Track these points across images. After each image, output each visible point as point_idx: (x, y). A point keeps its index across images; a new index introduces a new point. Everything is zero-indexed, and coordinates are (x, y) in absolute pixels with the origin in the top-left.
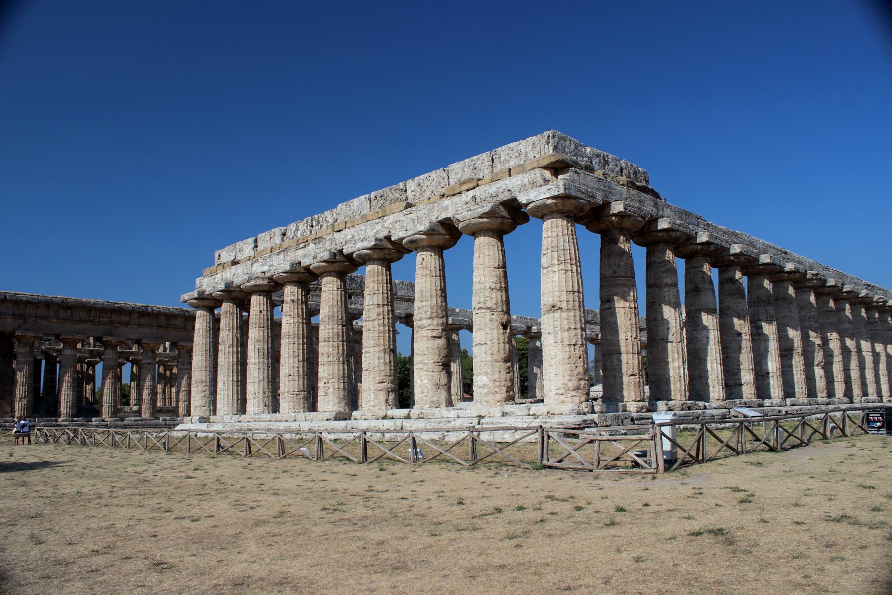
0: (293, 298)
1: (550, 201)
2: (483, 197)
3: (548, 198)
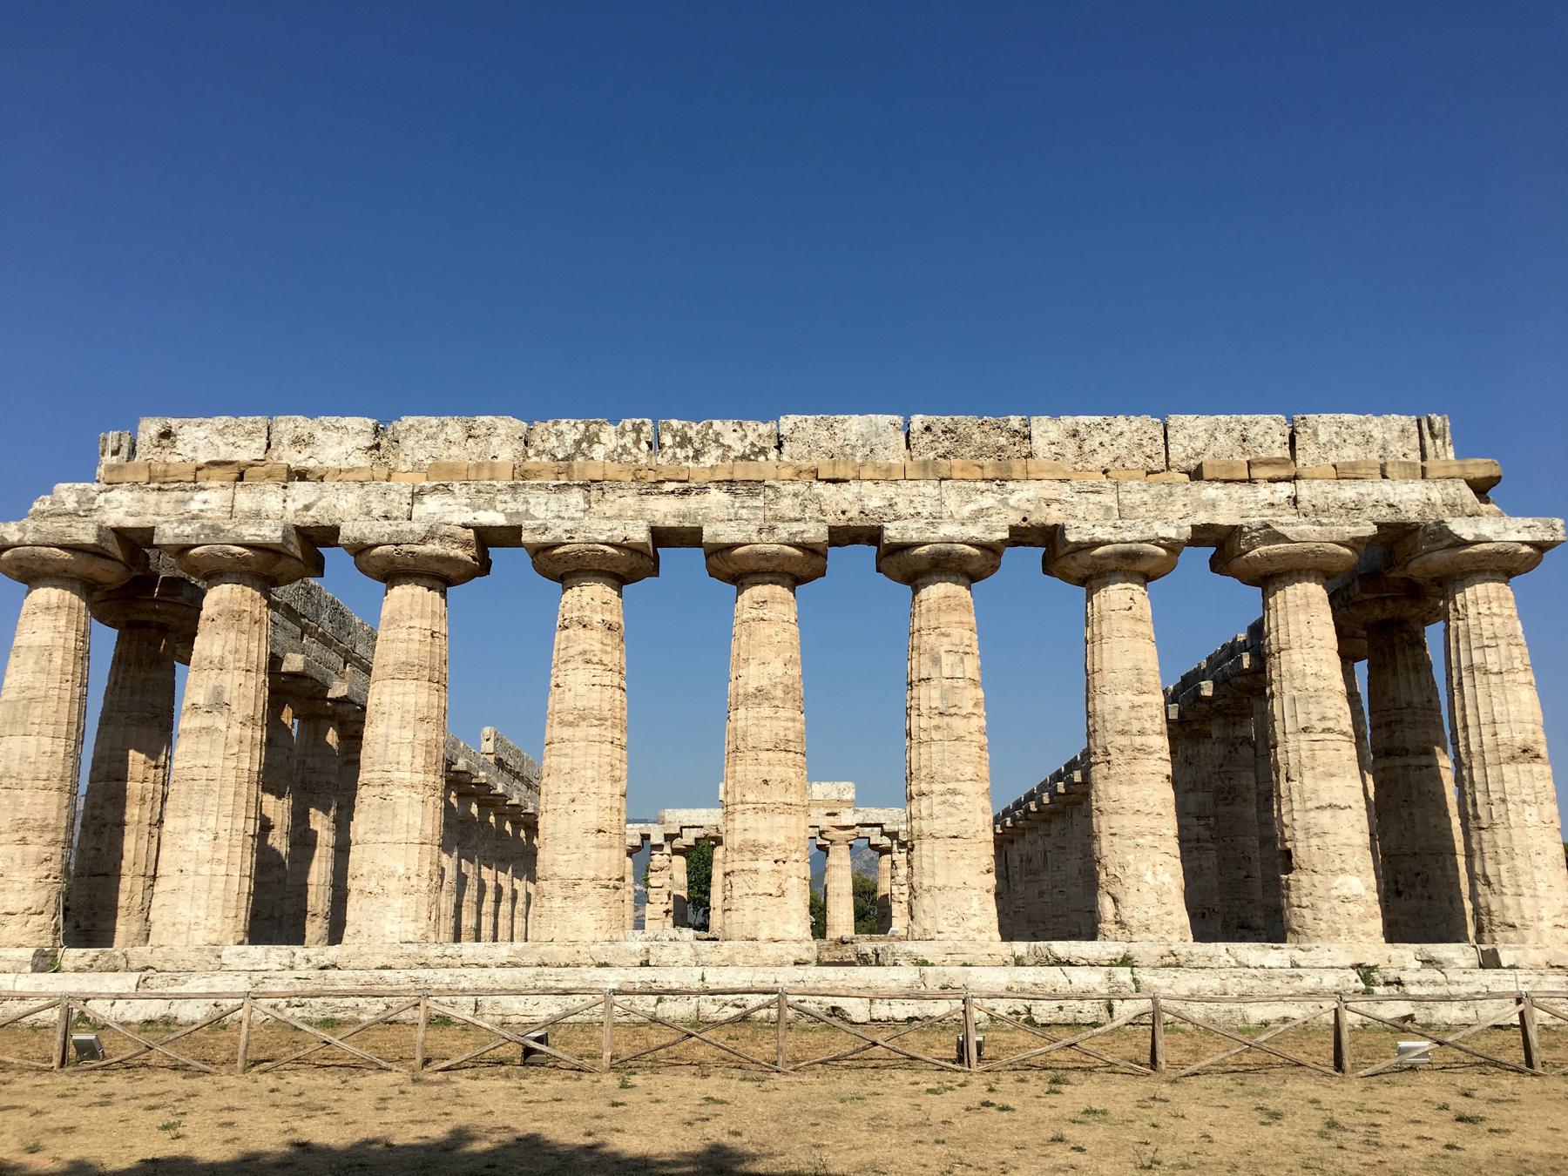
0: (608, 617)
1: (1526, 549)
2: (1320, 502)
3: (1524, 543)
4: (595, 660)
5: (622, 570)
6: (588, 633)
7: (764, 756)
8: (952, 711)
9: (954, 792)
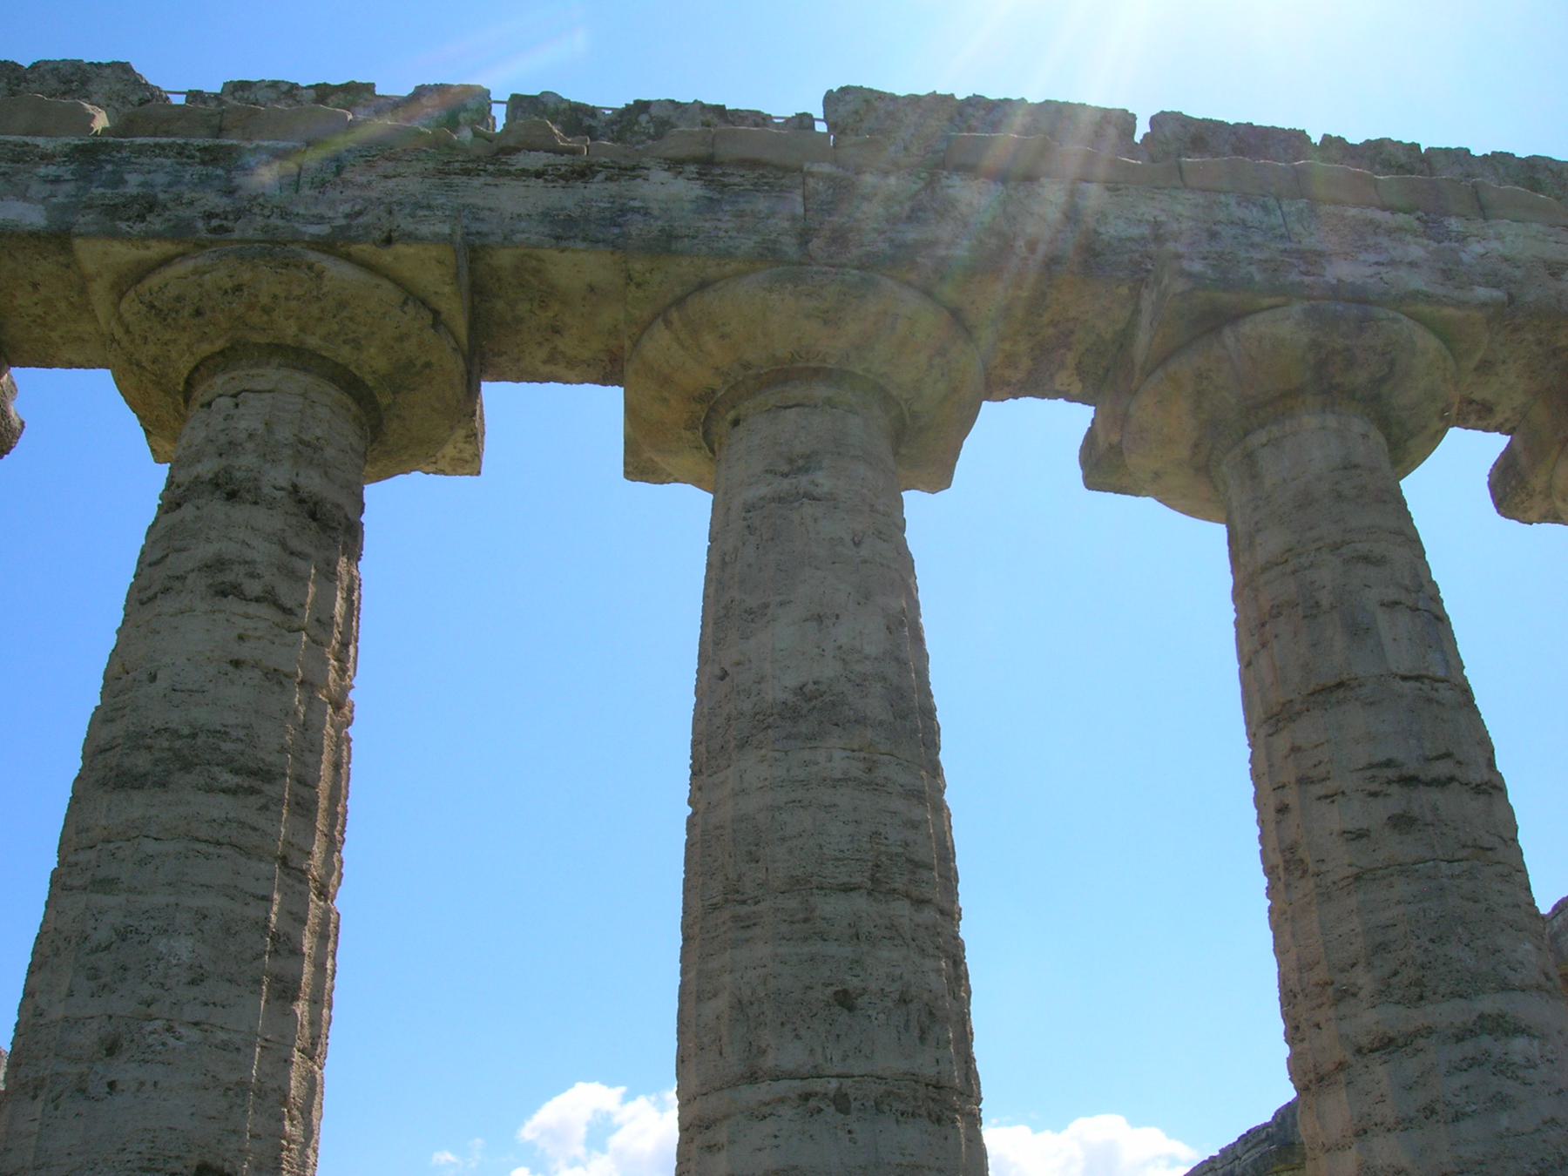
0: (312, 482)
4: (253, 587)
5: (372, 361)
6: (240, 513)
7: (832, 907)
8: (1442, 769)
9: (1501, 1026)
